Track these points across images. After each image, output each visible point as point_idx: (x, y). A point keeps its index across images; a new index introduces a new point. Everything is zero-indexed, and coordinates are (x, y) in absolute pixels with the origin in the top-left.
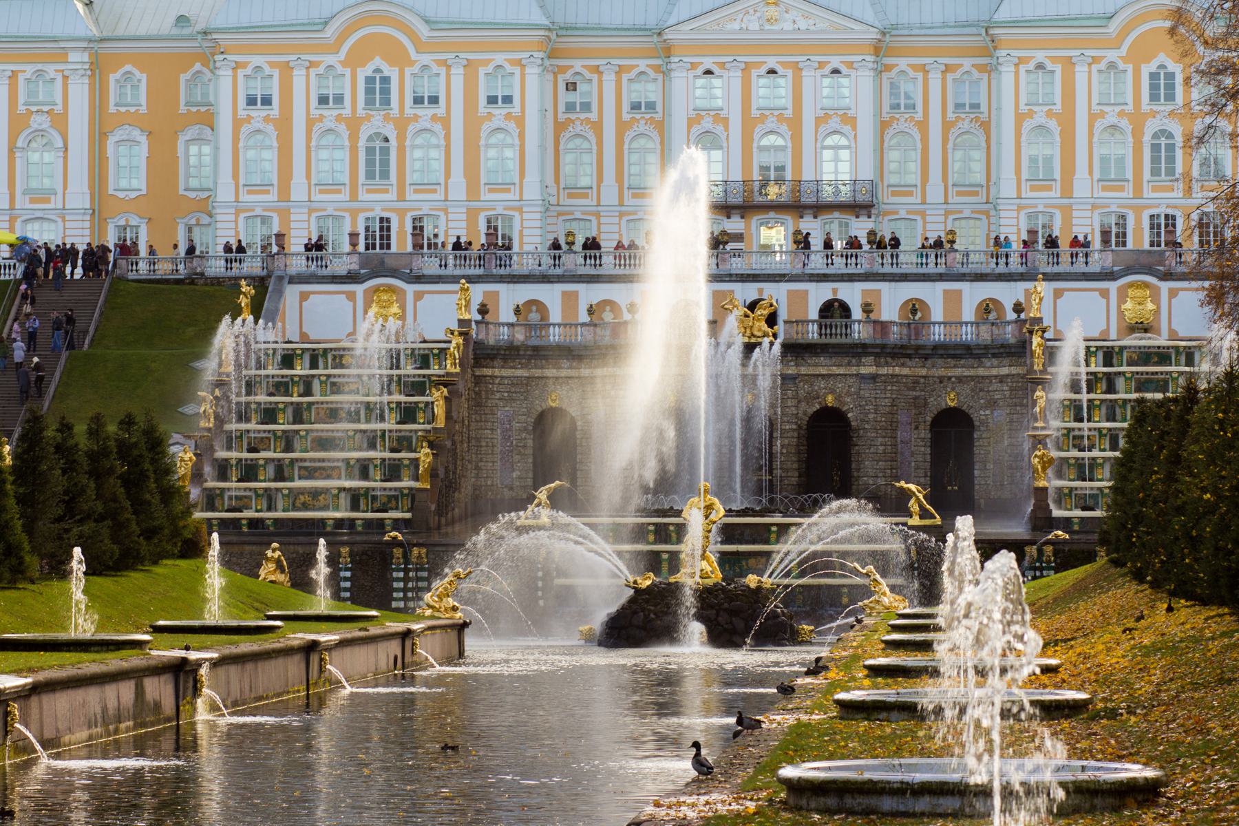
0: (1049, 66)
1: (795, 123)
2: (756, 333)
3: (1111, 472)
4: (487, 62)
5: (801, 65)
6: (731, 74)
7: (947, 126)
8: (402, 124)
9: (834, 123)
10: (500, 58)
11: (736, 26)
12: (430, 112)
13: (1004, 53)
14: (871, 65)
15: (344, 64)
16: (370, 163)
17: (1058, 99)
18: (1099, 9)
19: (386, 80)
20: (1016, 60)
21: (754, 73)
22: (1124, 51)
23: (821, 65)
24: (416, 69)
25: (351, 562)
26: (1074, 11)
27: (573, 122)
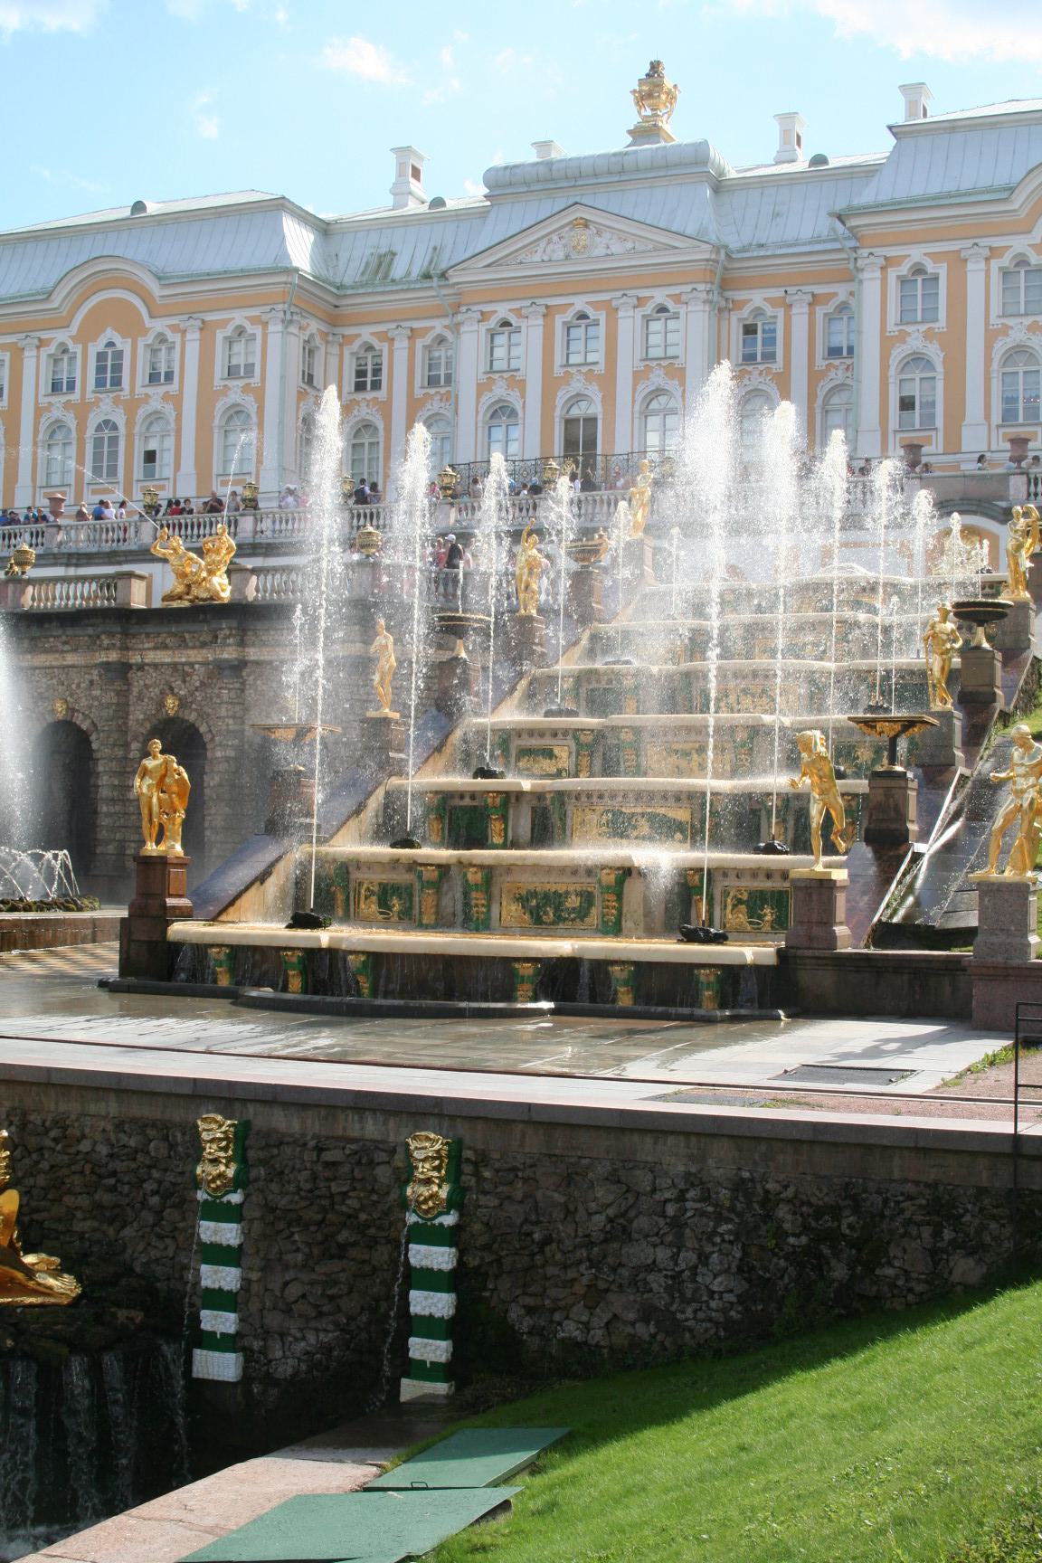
0: (931, 268)
1: (607, 381)
4: (224, 323)
6: (531, 322)
8: (131, 407)
9: (657, 379)
10: (239, 317)
11: (537, 258)
12: (161, 390)
13: (865, 252)
14: (704, 296)
17: (942, 314)
18: (1002, 179)
19: (119, 355)
20: (881, 261)
21: (559, 321)
24: (150, 339)
26: (966, 185)
27: (358, 403)
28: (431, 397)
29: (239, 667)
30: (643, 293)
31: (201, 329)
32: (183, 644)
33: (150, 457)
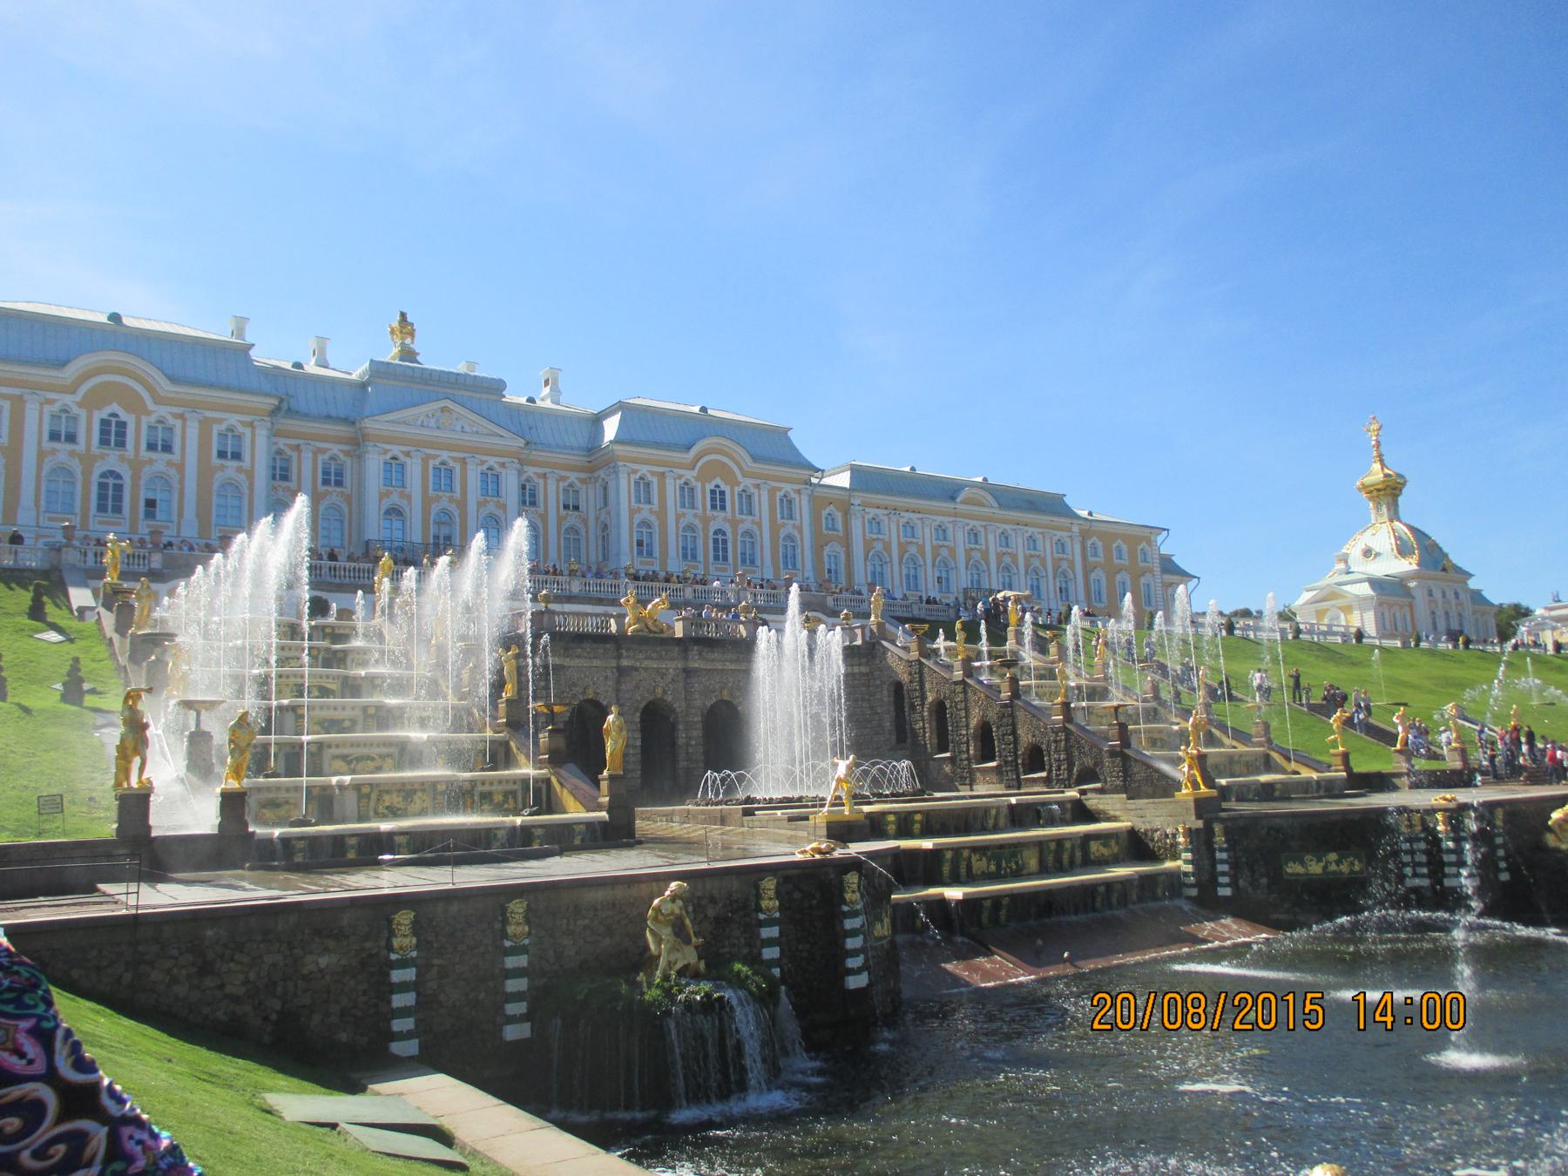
0: (650, 477)
2: (653, 628)
3: (975, 750)
5: (468, 460)
6: (414, 461)
7: (560, 520)
10: (233, 419)
13: (620, 464)
15: (80, 405)
16: (102, 497)
19: (122, 425)
21: (431, 463)
22: (695, 473)
23: (483, 462)
24: (153, 419)
25: (780, 909)
28: (331, 493)
29: (696, 670)
30: (484, 458)
31: (200, 422)
32: (660, 658)
33: (151, 504)
